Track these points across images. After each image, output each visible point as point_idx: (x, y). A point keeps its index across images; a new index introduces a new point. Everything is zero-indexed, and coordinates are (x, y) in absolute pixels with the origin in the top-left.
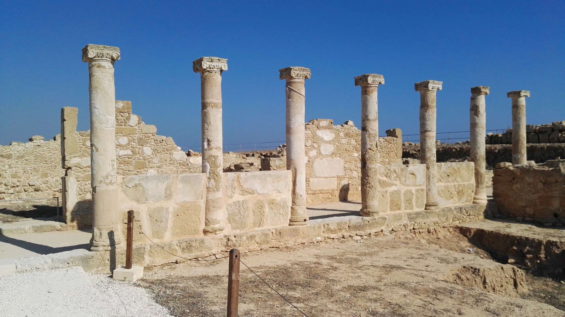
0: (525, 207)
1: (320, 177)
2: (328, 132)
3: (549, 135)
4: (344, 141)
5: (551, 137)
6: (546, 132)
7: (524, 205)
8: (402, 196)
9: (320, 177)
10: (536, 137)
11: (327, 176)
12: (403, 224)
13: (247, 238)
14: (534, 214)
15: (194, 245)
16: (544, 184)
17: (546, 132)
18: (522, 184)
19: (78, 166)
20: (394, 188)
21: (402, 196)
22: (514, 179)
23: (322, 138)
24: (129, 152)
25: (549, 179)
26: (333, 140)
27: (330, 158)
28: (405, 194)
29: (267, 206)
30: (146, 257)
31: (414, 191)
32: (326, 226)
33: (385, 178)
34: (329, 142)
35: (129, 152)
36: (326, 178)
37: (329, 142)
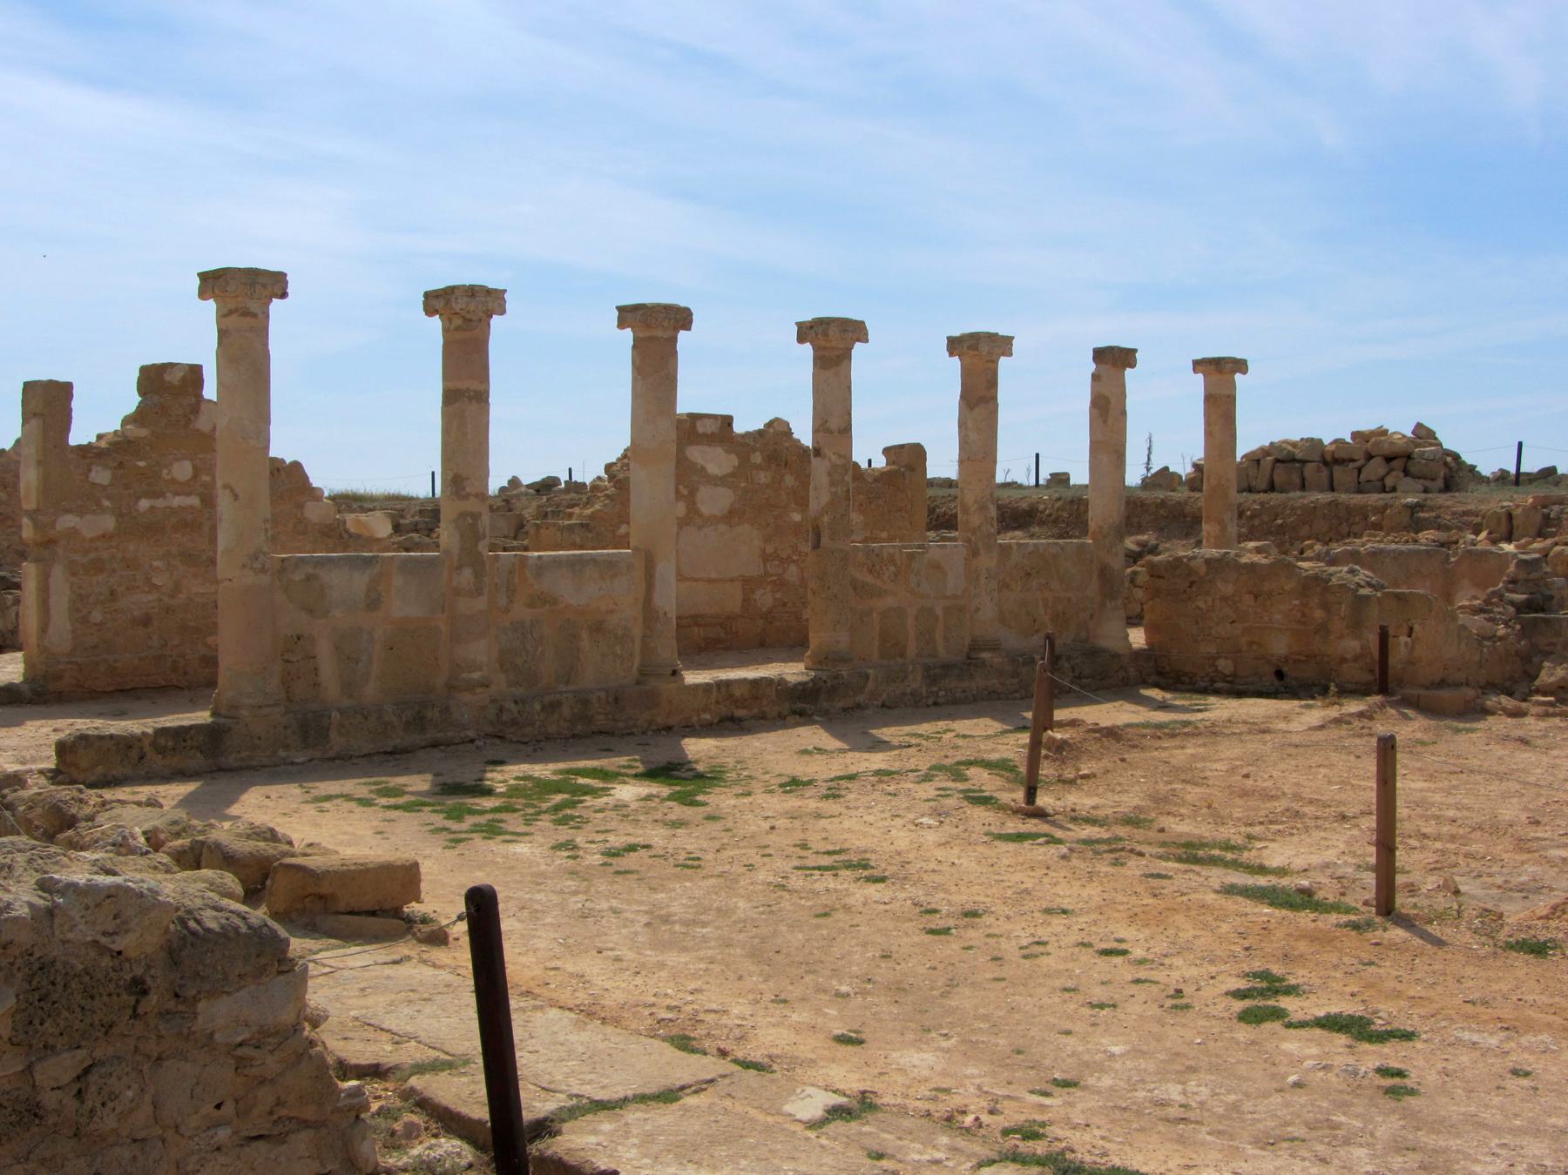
0: (1215, 658)
1: (696, 580)
2: (719, 451)
3: (1360, 470)
4: (763, 477)
5: (1363, 477)
6: (1353, 460)
7: (1212, 649)
8: (910, 621)
9: (696, 580)
10: (1325, 473)
11: (713, 576)
12: (908, 690)
13: (543, 708)
14: (1235, 675)
15: (429, 714)
16: (1256, 597)
17: (1353, 460)
18: (1209, 599)
19: (73, 533)
20: (890, 601)
21: (910, 621)
22: (1192, 584)
23: (703, 468)
24: (194, 501)
25: (1266, 586)
26: (733, 475)
27: (722, 528)
28: (916, 618)
29: (585, 635)
30: (333, 735)
31: (939, 611)
32: (723, 689)
33: (869, 579)
34: (722, 481)
35: (194, 501)
36: (710, 581)
37: (722, 481)
